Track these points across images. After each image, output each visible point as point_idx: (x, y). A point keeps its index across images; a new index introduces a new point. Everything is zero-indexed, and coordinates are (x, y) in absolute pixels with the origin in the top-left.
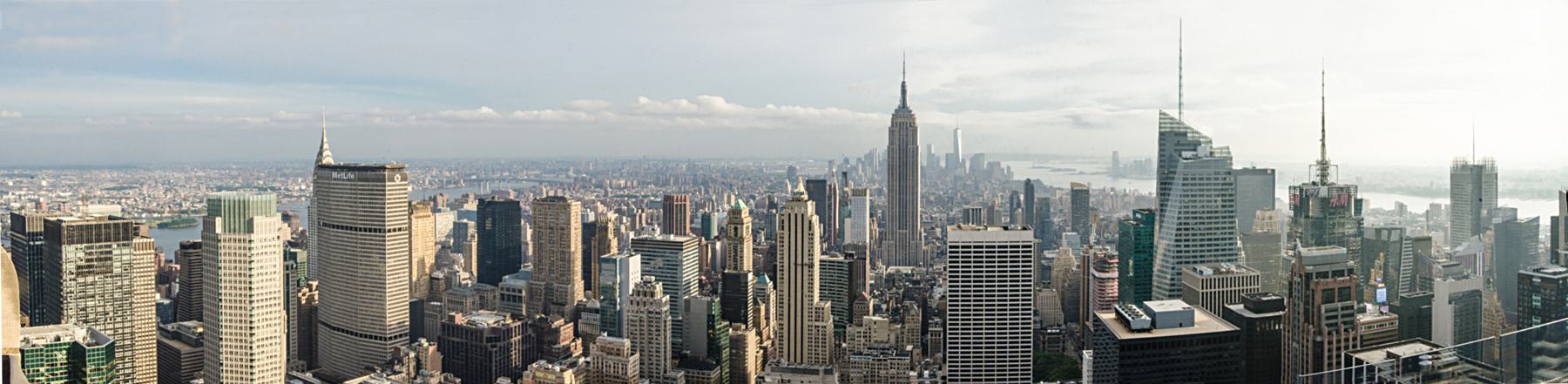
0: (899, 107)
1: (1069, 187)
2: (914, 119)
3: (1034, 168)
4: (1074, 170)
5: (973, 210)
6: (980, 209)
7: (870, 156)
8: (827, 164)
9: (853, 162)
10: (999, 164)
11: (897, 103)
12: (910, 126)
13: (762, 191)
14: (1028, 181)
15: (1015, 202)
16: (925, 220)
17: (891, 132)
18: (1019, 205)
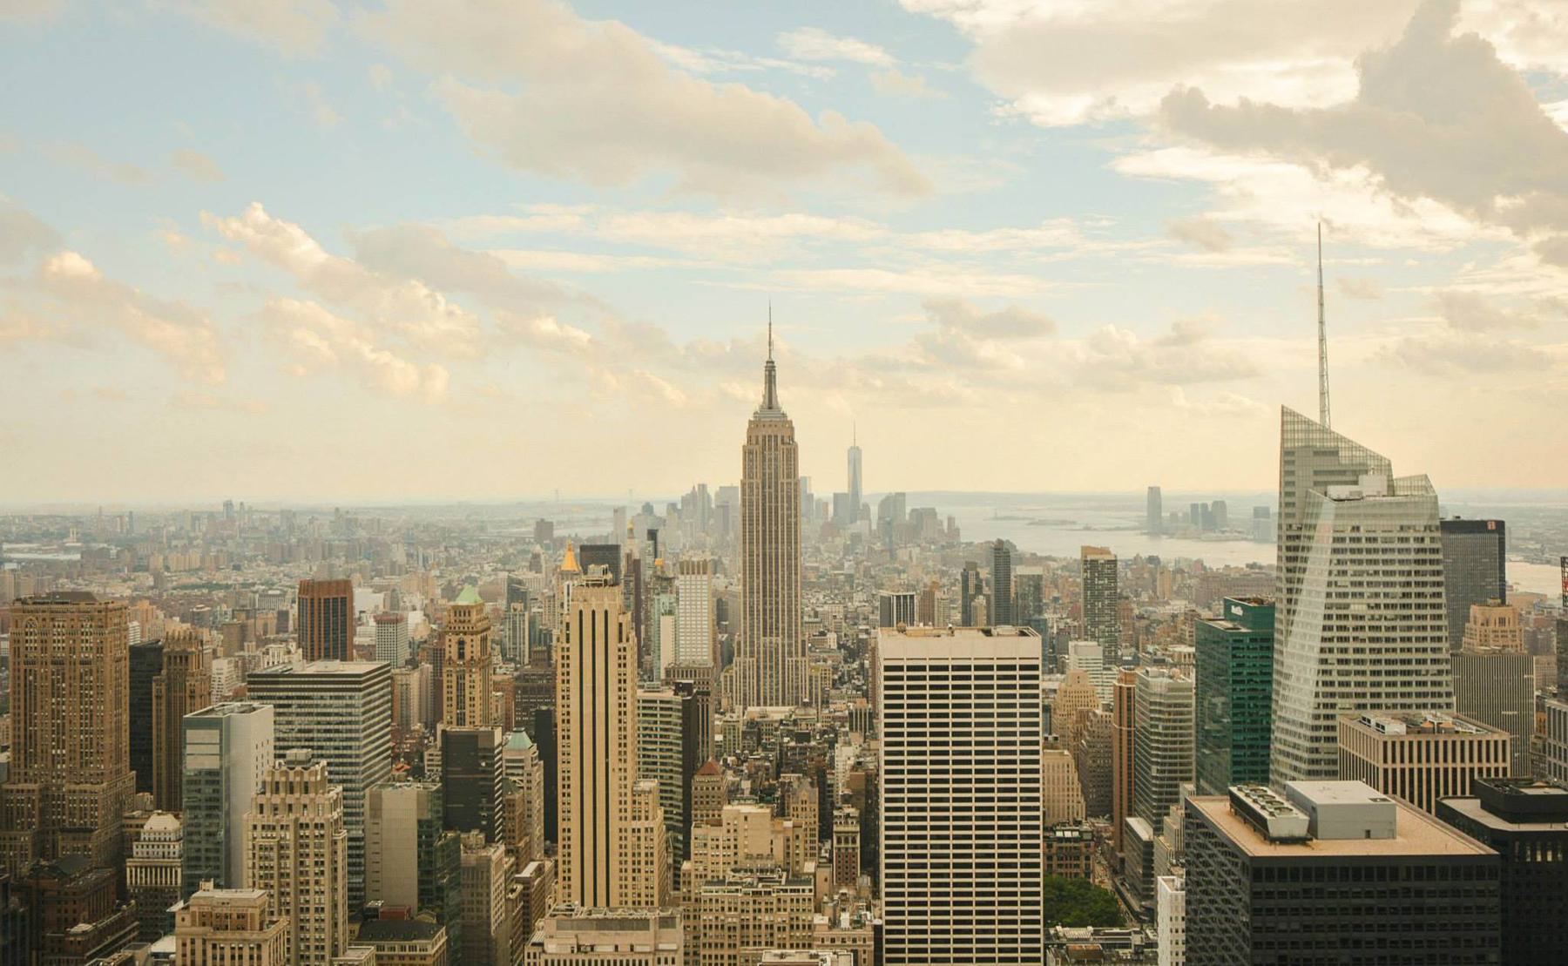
0: (762, 407)
1: (1078, 556)
2: (792, 429)
3: (996, 518)
4: (1074, 523)
5: (898, 597)
6: (912, 597)
7: (690, 500)
8: (611, 514)
9: (660, 511)
10: (932, 513)
11: (761, 400)
12: (783, 443)
13: (487, 568)
14: (1000, 542)
15: (972, 583)
16: (806, 619)
17: (748, 454)
18: (979, 589)
